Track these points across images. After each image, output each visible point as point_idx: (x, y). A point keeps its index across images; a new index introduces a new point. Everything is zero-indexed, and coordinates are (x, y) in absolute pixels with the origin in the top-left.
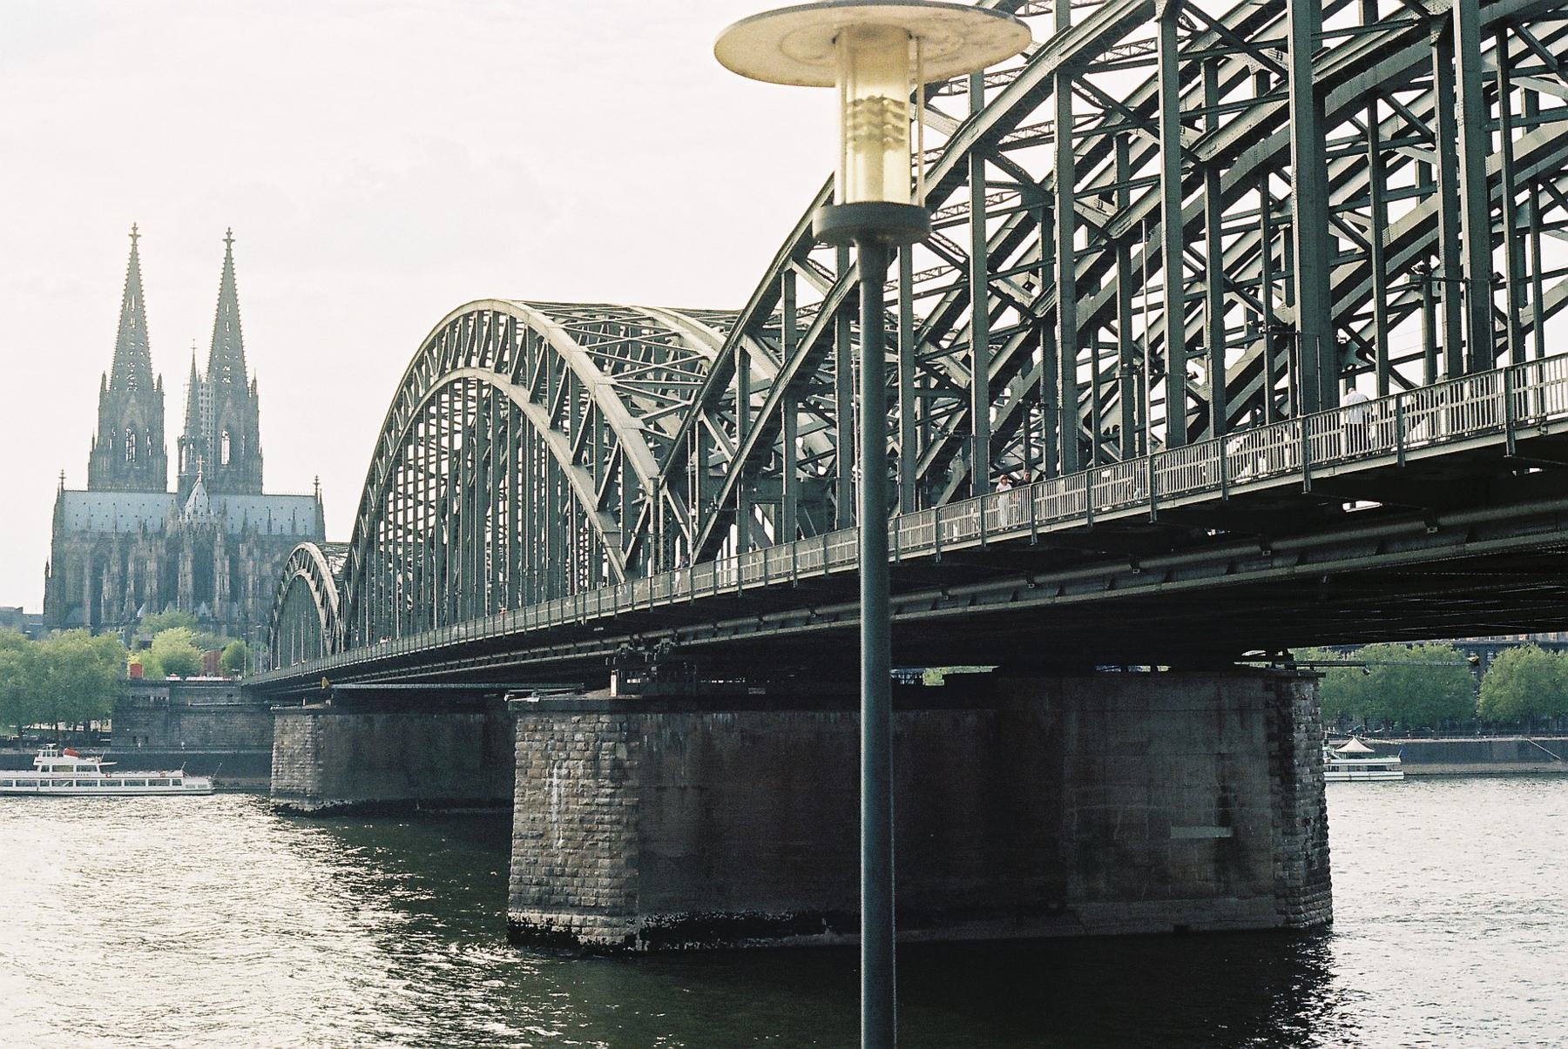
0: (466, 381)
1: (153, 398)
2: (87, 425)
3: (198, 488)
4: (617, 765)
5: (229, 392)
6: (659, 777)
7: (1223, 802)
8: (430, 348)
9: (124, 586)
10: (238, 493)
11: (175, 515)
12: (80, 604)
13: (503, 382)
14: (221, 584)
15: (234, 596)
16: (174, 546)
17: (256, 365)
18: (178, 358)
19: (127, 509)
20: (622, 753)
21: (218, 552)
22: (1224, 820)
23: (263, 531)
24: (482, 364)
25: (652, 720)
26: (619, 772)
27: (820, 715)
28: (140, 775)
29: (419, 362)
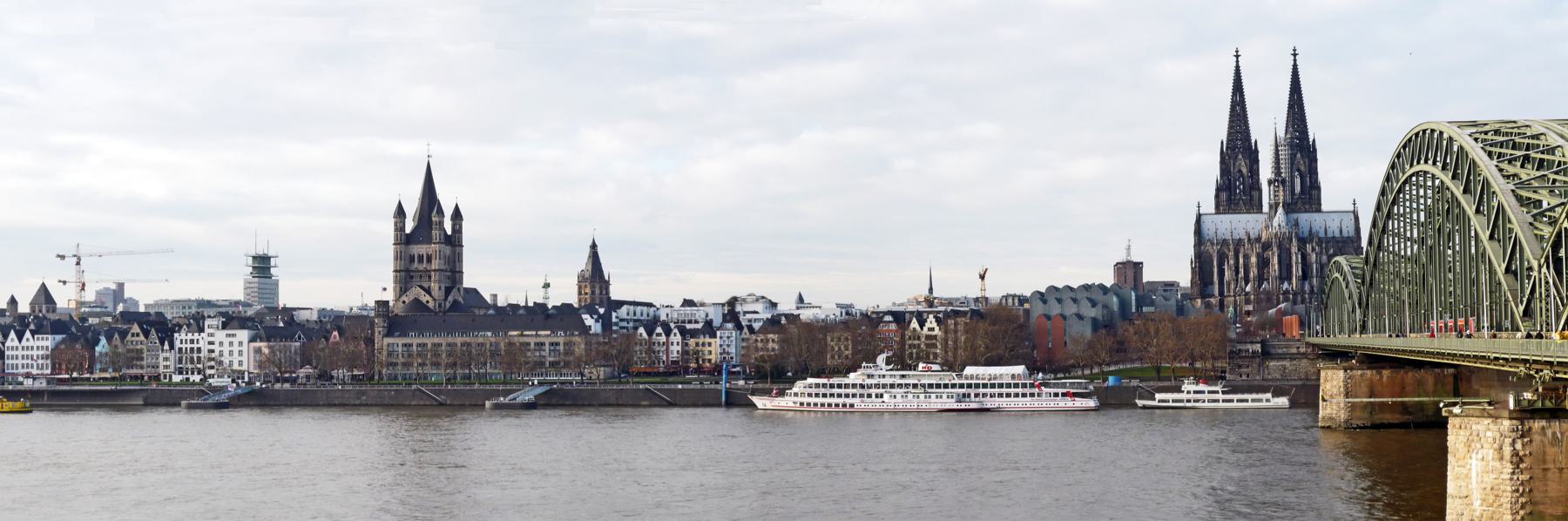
0: (1426, 173)
3: (1280, 210)
4: (1515, 453)
5: (1300, 147)
6: (1544, 461)
8: (1404, 147)
9: (1237, 272)
11: (1267, 227)
13: (1446, 178)
15: (1305, 276)
16: (1267, 246)
17: (1314, 130)
18: (1267, 127)
20: (1519, 446)
21: (1294, 249)
23: (1322, 235)
24: (1434, 163)
25: (1537, 425)
26: (1517, 459)
29: (1398, 156)
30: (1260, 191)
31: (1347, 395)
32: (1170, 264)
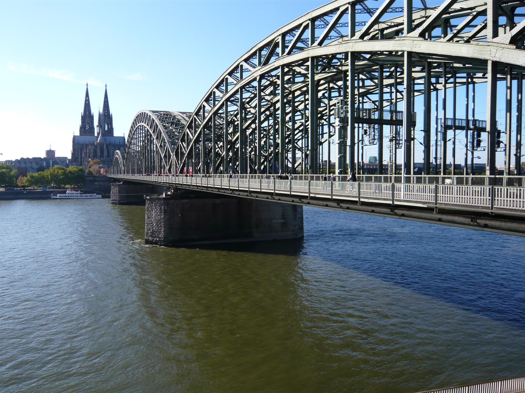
1: (91, 118)
2: (79, 123)
4: (165, 210)
5: (106, 117)
7: (283, 215)
10: (109, 136)
12: (78, 158)
14: (105, 154)
17: (112, 111)
18: (96, 110)
19: (87, 139)
20: (166, 208)
21: (105, 148)
22: (283, 219)
27: (205, 200)
28: (88, 195)
30: (94, 129)
31: (119, 193)
32: (65, 151)
